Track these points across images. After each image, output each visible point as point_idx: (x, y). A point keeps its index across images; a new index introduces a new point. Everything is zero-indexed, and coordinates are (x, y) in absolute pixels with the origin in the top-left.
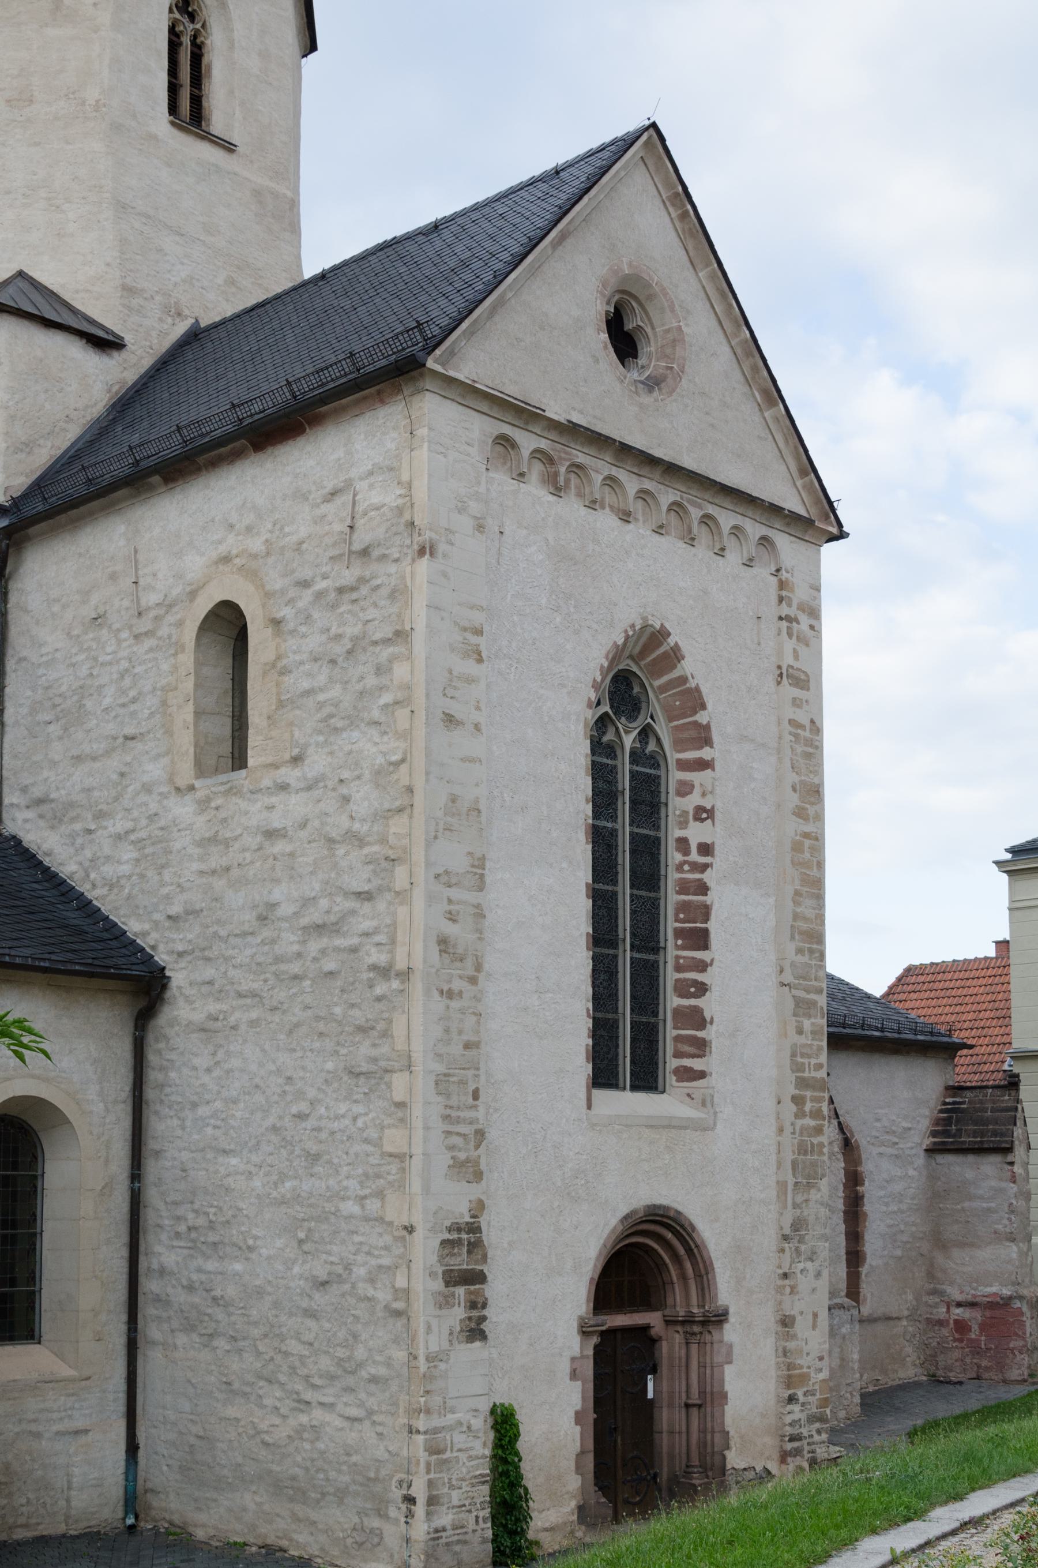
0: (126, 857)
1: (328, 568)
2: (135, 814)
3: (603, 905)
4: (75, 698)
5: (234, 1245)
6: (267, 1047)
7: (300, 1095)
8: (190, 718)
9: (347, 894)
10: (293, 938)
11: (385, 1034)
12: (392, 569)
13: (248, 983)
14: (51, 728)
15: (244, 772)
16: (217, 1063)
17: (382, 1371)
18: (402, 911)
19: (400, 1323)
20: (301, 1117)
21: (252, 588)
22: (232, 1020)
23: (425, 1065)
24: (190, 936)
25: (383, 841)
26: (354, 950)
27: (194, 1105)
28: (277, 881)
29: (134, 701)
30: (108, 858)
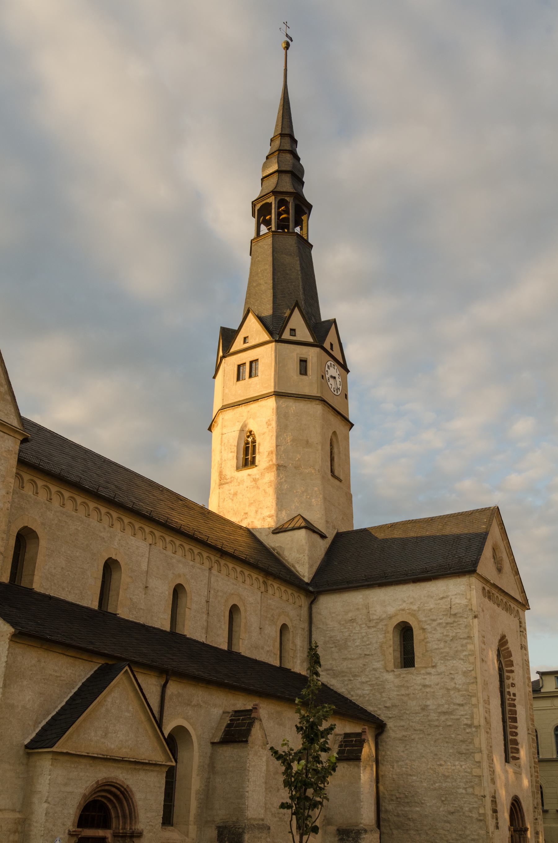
0: (366, 689)
1: (442, 617)
2: (370, 676)
4: (343, 641)
5: (416, 802)
6: (426, 745)
7: (440, 759)
8: (392, 652)
9: (454, 704)
10: (435, 715)
11: (472, 742)
12: (465, 620)
13: (418, 727)
14: (333, 649)
15: (414, 668)
16: (406, 749)
17: (476, 837)
18: (475, 710)
19: (481, 824)
20: (441, 765)
21: (414, 619)
22: (412, 737)
24: (394, 713)
25: (467, 690)
26: (458, 719)
27: (397, 762)
28: (429, 699)
29: (368, 645)
30: (359, 689)
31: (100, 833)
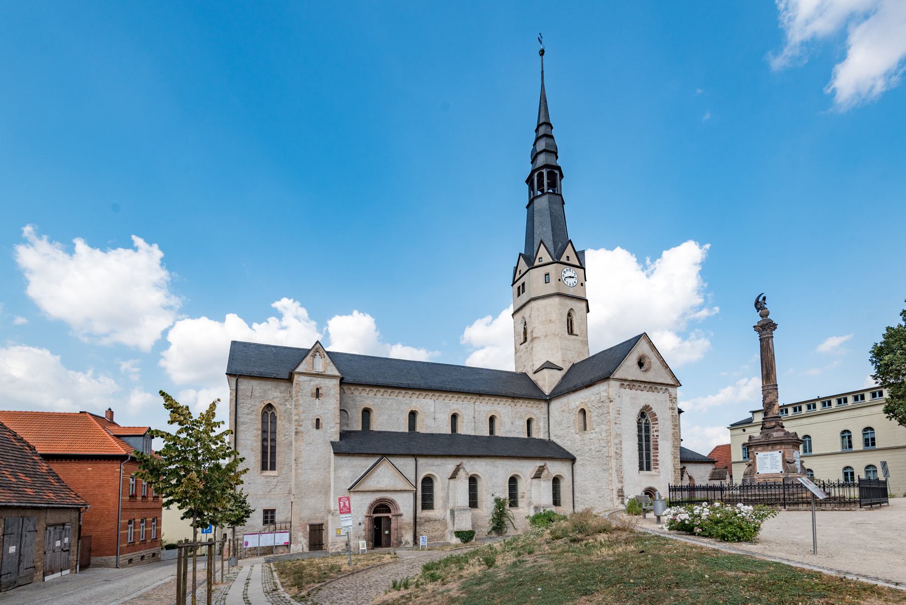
3: (640, 445)
23: (614, 469)
31: (386, 515)
